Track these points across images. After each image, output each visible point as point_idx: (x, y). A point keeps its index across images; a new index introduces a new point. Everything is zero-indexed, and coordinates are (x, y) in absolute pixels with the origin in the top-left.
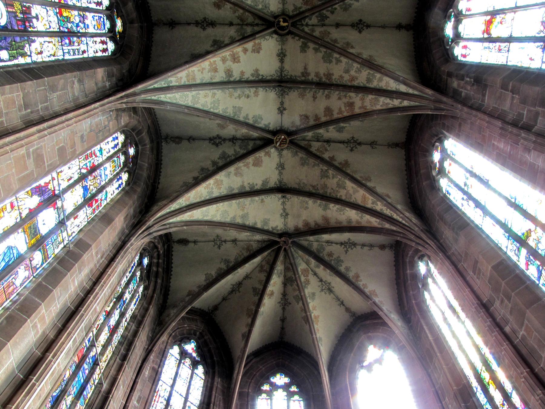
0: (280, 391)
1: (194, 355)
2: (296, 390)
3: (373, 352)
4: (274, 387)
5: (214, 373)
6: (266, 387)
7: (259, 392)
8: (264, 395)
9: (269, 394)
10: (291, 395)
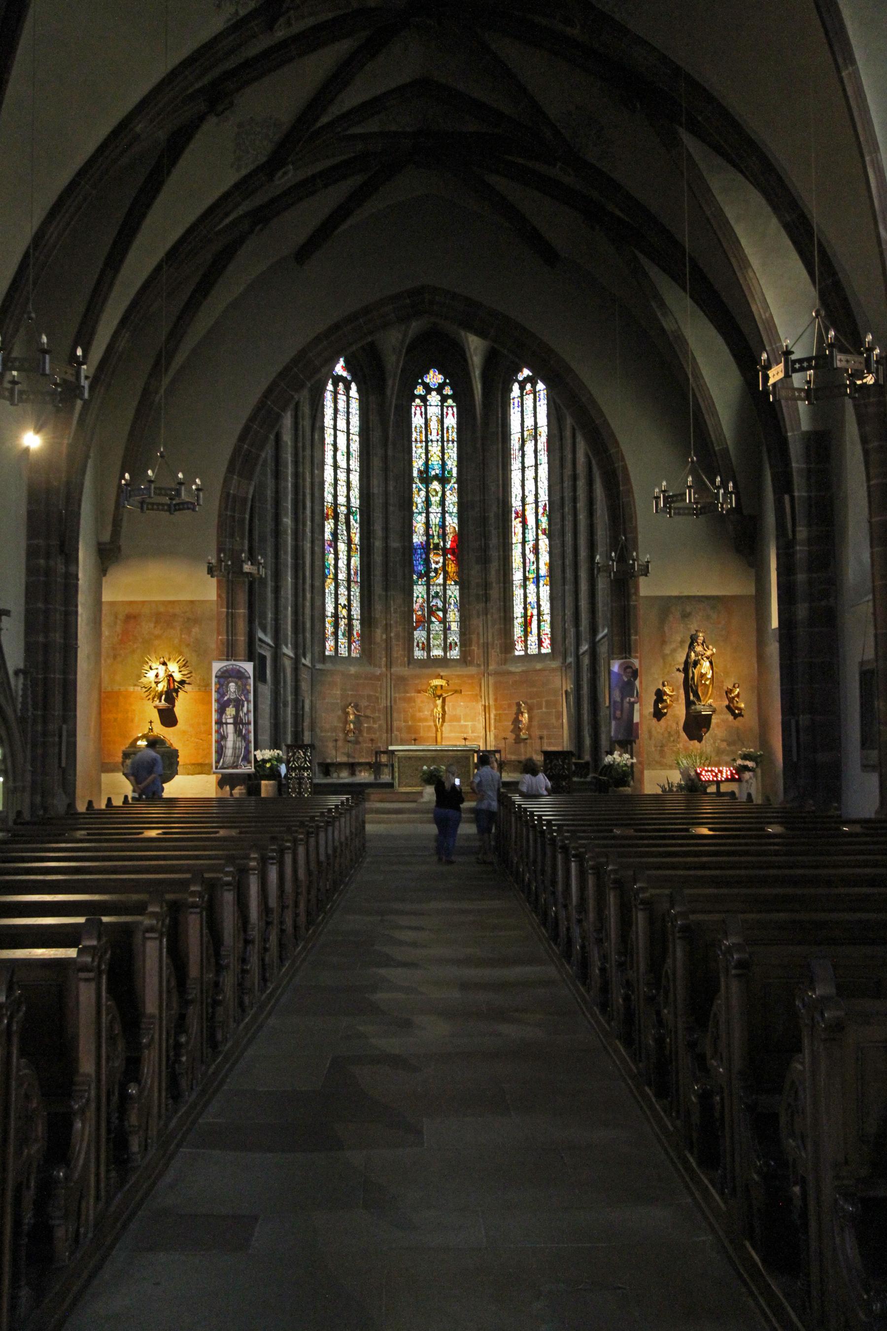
0: (434, 393)
1: (345, 374)
2: (450, 393)
6: (420, 390)
8: (418, 401)
9: (424, 399)
10: (444, 399)
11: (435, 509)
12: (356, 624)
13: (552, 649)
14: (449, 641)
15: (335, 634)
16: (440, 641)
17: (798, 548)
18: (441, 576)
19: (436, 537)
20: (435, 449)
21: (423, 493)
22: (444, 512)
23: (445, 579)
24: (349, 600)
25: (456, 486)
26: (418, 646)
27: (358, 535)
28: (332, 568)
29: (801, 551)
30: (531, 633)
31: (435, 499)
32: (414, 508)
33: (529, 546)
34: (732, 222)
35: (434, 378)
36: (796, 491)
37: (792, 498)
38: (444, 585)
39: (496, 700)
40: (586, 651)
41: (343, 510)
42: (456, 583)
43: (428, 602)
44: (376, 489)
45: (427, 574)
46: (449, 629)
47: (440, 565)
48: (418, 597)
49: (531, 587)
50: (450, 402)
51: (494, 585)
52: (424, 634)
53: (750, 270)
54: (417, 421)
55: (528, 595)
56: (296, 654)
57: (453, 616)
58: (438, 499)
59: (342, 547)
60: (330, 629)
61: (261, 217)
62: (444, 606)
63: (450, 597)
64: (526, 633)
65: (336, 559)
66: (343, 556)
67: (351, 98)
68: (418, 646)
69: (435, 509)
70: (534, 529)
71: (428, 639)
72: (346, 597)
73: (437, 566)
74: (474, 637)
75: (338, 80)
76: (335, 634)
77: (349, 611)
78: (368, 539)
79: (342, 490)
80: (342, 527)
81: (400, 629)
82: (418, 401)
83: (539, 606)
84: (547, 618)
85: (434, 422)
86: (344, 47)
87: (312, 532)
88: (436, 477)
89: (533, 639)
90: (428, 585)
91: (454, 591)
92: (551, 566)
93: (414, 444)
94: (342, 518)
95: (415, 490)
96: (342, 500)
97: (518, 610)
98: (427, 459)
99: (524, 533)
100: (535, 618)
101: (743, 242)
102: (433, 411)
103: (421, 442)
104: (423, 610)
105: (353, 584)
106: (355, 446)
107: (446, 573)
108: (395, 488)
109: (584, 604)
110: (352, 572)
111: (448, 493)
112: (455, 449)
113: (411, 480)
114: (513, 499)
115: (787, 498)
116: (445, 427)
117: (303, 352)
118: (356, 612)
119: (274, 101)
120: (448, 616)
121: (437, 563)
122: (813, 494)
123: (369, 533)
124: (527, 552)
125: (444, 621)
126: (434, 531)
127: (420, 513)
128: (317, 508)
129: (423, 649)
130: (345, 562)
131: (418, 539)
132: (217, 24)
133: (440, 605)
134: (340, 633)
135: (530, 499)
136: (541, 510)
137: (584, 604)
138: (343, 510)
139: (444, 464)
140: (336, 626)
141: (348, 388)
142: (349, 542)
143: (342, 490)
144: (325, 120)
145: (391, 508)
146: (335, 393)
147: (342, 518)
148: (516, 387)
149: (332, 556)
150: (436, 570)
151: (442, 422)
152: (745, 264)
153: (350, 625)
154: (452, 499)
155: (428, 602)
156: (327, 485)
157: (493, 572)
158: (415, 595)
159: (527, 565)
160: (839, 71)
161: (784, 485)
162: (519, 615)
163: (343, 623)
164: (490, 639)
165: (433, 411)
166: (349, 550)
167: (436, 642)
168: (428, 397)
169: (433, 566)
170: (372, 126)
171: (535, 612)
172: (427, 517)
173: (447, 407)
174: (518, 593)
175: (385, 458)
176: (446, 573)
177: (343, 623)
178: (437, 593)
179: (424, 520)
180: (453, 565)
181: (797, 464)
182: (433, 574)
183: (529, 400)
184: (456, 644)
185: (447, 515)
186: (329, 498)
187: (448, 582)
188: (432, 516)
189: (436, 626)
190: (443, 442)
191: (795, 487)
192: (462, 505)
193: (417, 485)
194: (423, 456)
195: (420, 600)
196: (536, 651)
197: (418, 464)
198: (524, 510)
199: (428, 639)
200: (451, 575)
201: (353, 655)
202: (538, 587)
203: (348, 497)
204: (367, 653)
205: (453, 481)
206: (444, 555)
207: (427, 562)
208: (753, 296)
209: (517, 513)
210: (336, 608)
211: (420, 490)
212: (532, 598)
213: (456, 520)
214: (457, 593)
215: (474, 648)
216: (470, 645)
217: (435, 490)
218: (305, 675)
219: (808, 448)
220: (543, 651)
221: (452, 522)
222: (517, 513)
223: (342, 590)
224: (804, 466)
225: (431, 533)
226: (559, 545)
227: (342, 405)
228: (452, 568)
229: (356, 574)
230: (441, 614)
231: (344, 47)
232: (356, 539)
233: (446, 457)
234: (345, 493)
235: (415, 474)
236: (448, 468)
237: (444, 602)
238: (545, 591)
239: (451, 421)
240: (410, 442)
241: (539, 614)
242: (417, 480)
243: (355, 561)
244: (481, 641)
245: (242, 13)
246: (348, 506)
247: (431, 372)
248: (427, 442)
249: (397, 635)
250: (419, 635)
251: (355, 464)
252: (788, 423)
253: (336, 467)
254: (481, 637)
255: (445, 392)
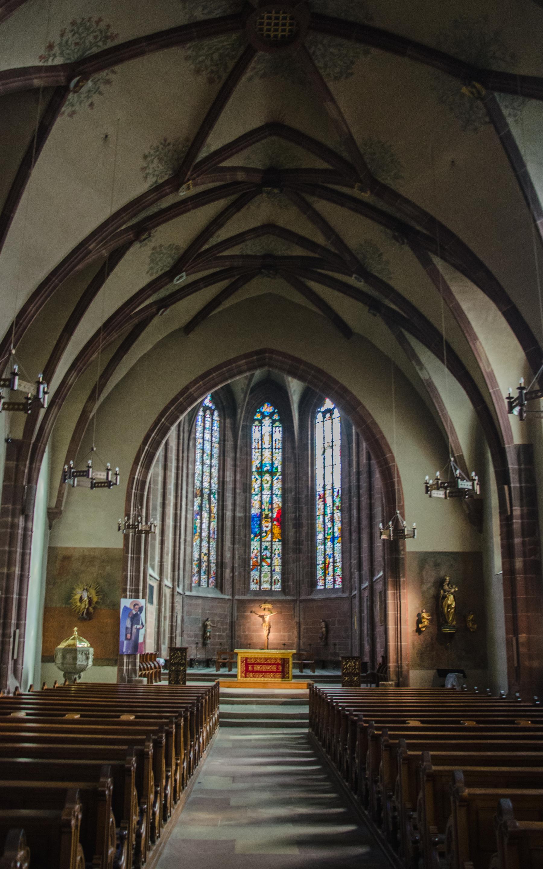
1: (210, 405)
3: (328, 404)
4: (264, 416)
5: (224, 415)
6: (258, 416)
7: (254, 421)
8: (257, 423)
9: (260, 422)
10: (274, 422)
11: (266, 492)
12: (213, 566)
13: (343, 585)
14: (274, 579)
15: (199, 572)
16: (268, 579)
17: (514, 521)
18: (270, 536)
19: (266, 510)
20: (267, 453)
21: (259, 482)
22: (272, 494)
23: (272, 538)
24: (209, 550)
25: (280, 477)
26: (253, 581)
27: (216, 508)
28: (198, 529)
29: (517, 523)
30: (328, 574)
31: (266, 486)
32: (253, 491)
33: (327, 518)
34: (466, 312)
35: (267, 409)
36: (512, 483)
37: (510, 488)
38: (272, 541)
39: (304, 618)
40: (367, 587)
41: (206, 491)
42: (279, 541)
43: (261, 553)
44: (229, 478)
45: (260, 534)
46: (274, 570)
47: (269, 528)
48: (254, 549)
49: (329, 544)
50: (277, 424)
51: (304, 542)
52: (258, 573)
53: (478, 342)
54: (256, 435)
55: (327, 549)
56: (173, 585)
57: (277, 561)
58: (268, 485)
59: (205, 515)
60: (196, 569)
61: (164, 304)
62: (271, 555)
63: (275, 550)
64: (325, 574)
65: (201, 523)
66: (205, 521)
67: (223, 234)
68: (253, 581)
69: (266, 492)
70: (331, 506)
71: (260, 577)
72: (207, 548)
73: (267, 529)
74: (291, 576)
75: (217, 223)
76: (199, 572)
77: (209, 557)
78: (223, 510)
79: (206, 478)
80: (206, 502)
81: (242, 570)
82: (257, 423)
83: (334, 557)
84: (339, 564)
85: (266, 436)
86: (221, 204)
87: (187, 505)
88: (267, 471)
89: (329, 578)
90: (261, 541)
91: (278, 546)
92: (342, 530)
93: (253, 450)
94: (206, 496)
95: (253, 480)
96: (206, 485)
97: (320, 559)
98: (262, 460)
99: (324, 509)
100: (331, 564)
101: (473, 324)
102: (266, 430)
103: (258, 449)
104: (257, 558)
105: (211, 540)
106: (216, 451)
107: (273, 534)
108: (241, 477)
109: (365, 556)
110: (211, 532)
111: (275, 482)
112: (280, 454)
113: (251, 473)
114: (317, 487)
115: (506, 487)
116: (274, 439)
117: (186, 389)
118: (213, 558)
119: (175, 235)
120: (273, 562)
121: (267, 527)
122: (523, 485)
123: (223, 505)
124: (327, 521)
125: (270, 565)
126: (266, 506)
127: (257, 494)
128: (190, 489)
129: (257, 583)
130: (207, 525)
131: (255, 511)
132: (143, 188)
133: (269, 555)
134: (202, 572)
135: (329, 487)
136: (336, 494)
137: (365, 556)
138: (206, 491)
139: (272, 464)
140: (200, 566)
141: (212, 414)
142: (210, 512)
143: (206, 478)
144: (206, 247)
145: (238, 491)
146: (204, 417)
147: (206, 496)
148: (320, 416)
149: (198, 521)
150: (266, 532)
151: (271, 436)
152: (475, 338)
153: (209, 566)
154: (277, 485)
155: (261, 553)
156: (196, 475)
157: (304, 534)
158: (252, 548)
159: (326, 529)
160: (535, 221)
161: (503, 477)
162: (321, 562)
163: (204, 565)
164: (301, 579)
165: (266, 430)
166: (210, 517)
167: (266, 579)
168: (263, 421)
169: (265, 529)
170: (235, 251)
171: (331, 560)
172: (261, 497)
173: (276, 427)
174: (320, 548)
175: (235, 459)
176: (273, 534)
177: (204, 565)
178: (267, 547)
179: (259, 499)
180: (278, 529)
181: (512, 465)
182: (264, 534)
183: (328, 423)
184: (278, 580)
185: (274, 496)
186: (198, 484)
187: (274, 540)
188: (264, 497)
189: (266, 569)
190: (272, 449)
191: (511, 480)
192: (284, 490)
193: (255, 475)
194: (260, 458)
195: (255, 551)
196: (331, 587)
197: (256, 463)
198: (324, 494)
199: (260, 577)
200: (276, 535)
201: (210, 586)
202: (333, 544)
203: (210, 482)
204: (220, 586)
205: (278, 474)
206: (272, 522)
207: (260, 526)
208: (480, 358)
209: (320, 495)
210: (200, 555)
211: (257, 480)
212: (329, 552)
213: (280, 500)
214: (280, 547)
215: (291, 583)
216: (288, 582)
217: (266, 480)
218: (178, 599)
219: (518, 455)
220: (337, 587)
221: (277, 501)
222: (320, 495)
223: (205, 544)
224: (517, 467)
225: (263, 507)
226: (347, 517)
227: (208, 424)
228: (277, 530)
229: (214, 533)
230: (269, 561)
231: (221, 204)
232: (215, 510)
233: (274, 459)
234: (209, 480)
235: (254, 469)
236: (275, 466)
237: (271, 553)
238: (338, 546)
239: (278, 436)
240: (251, 449)
241: (334, 562)
242: (255, 473)
243: (214, 525)
244: (295, 579)
245: (161, 181)
246: (210, 490)
247: (266, 405)
248: (262, 449)
249: (240, 574)
250: (254, 574)
251: (215, 462)
252: (505, 439)
253: (203, 464)
254: (295, 577)
255: (274, 418)
